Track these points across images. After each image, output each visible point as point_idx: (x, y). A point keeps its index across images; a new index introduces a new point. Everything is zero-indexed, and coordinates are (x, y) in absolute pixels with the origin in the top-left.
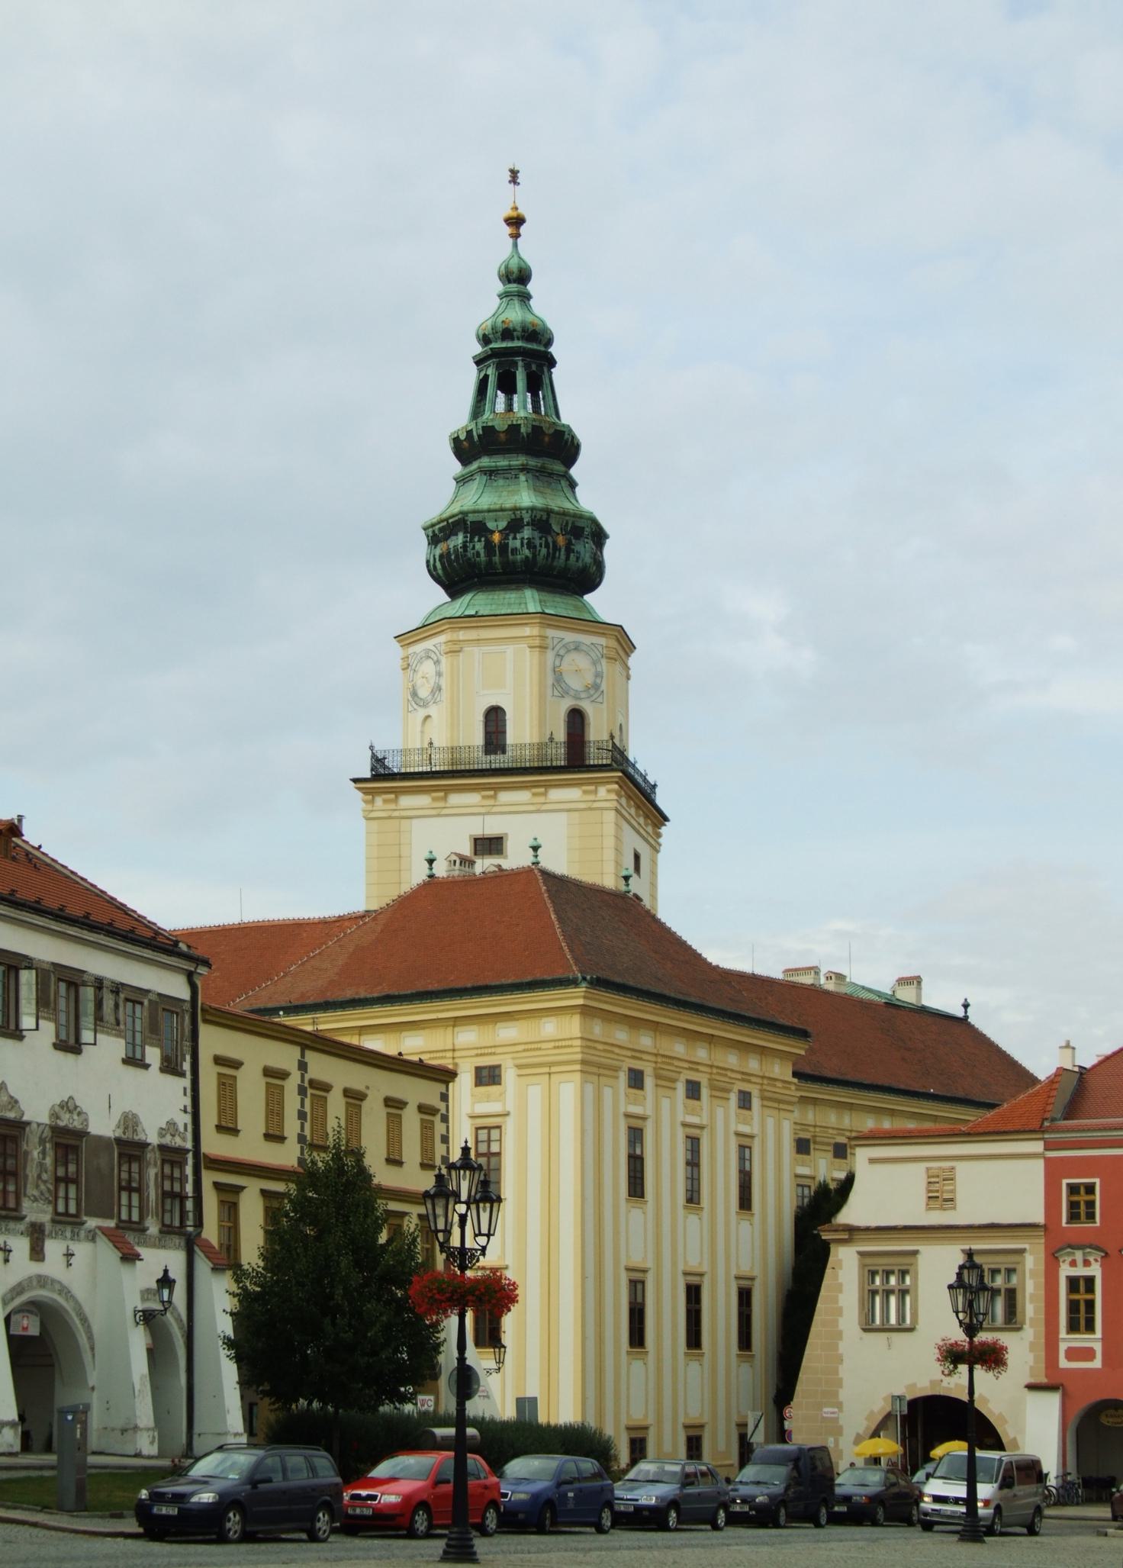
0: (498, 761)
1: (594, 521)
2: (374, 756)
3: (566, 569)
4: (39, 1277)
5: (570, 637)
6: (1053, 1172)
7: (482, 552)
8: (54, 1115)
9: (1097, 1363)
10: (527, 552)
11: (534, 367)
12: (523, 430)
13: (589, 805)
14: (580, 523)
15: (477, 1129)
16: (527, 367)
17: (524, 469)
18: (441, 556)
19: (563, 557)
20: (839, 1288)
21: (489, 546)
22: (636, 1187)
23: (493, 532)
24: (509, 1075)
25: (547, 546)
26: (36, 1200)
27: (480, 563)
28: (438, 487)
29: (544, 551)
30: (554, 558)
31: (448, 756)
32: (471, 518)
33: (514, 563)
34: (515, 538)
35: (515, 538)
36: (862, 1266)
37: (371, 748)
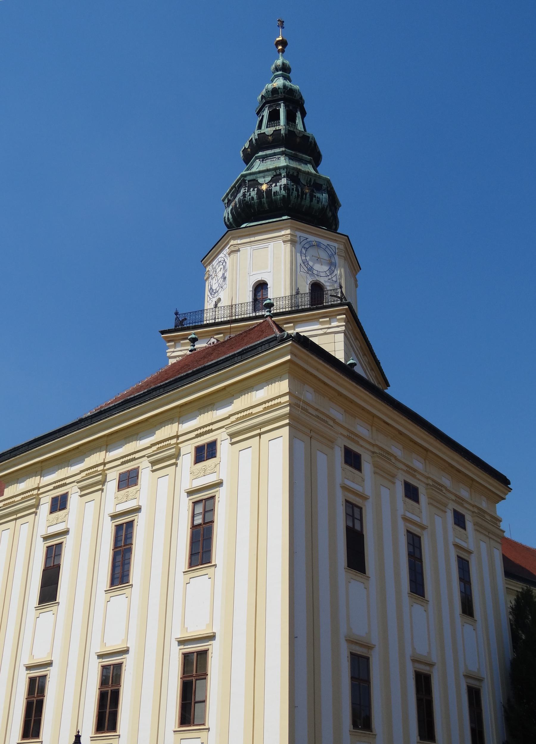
1: (328, 182)
2: (177, 318)
10: (283, 192)
11: (291, 108)
12: (283, 132)
13: (325, 330)
14: (321, 182)
15: (195, 503)
16: (286, 106)
17: (282, 153)
18: (231, 210)
21: (260, 192)
22: (356, 560)
23: (262, 184)
25: (297, 190)
29: (295, 193)
30: (302, 198)
32: (248, 178)
33: (276, 201)
35: (276, 186)
37: (176, 314)
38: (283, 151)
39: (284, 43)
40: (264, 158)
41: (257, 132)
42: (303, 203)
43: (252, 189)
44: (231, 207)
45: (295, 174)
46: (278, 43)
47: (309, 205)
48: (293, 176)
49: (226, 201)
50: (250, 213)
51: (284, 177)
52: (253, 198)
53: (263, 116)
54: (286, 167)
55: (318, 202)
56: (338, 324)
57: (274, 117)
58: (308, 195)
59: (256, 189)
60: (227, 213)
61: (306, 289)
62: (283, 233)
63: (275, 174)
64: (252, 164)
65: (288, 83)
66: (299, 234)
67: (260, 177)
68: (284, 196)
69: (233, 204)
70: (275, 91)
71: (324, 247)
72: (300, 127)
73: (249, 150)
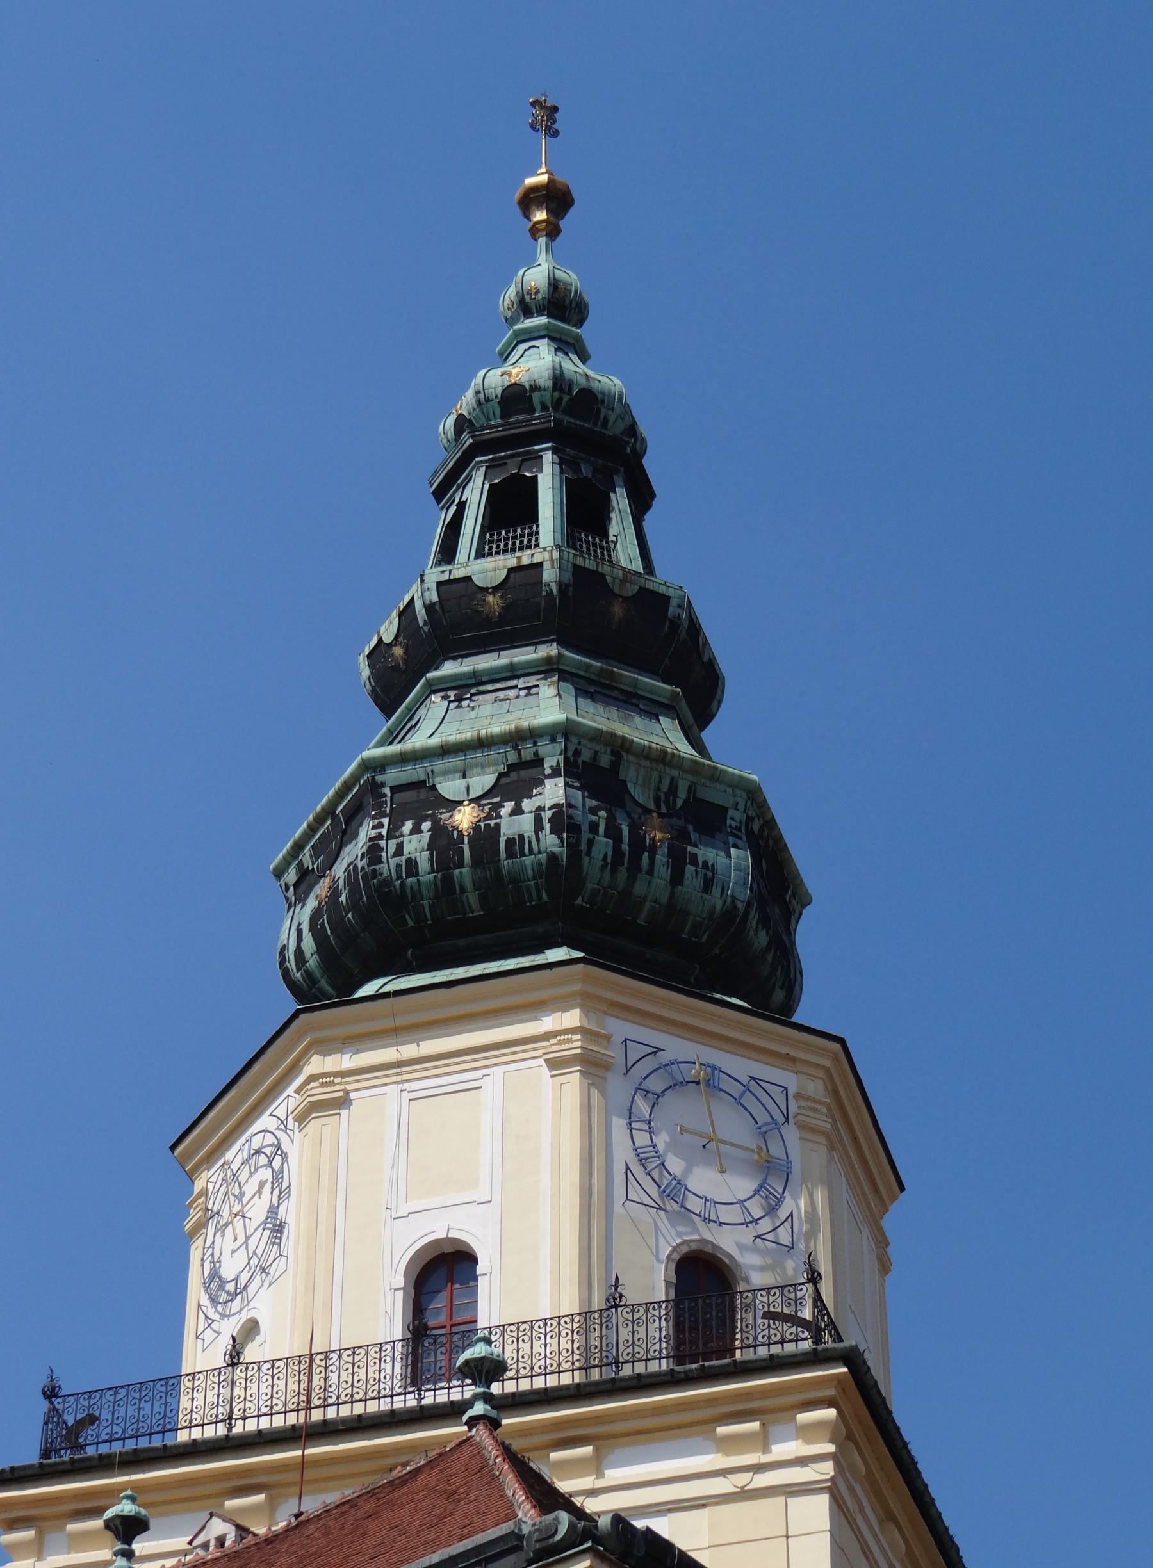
1: (753, 795)
3: (673, 909)
7: (423, 860)
10: (550, 841)
12: (549, 575)
13: (741, 1479)
16: (565, 464)
17: (547, 668)
18: (315, 916)
19: (663, 871)
21: (444, 842)
23: (454, 805)
25: (613, 832)
27: (417, 894)
31: (288, 1387)
32: (393, 776)
33: (516, 879)
34: (517, 811)
35: (517, 811)
37: (51, 1393)
38: (548, 660)
39: (556, 198)
40: (463, 689)
41: (434, 575)
42: (639, 888)
43: (408, 826)
44: (311, 904)
45: (605, 761)
46: (530, 199)
47: (664, 900)
48: (597, 768)
49: (291, 876)
50: (399, 933)
51: (555, 773)
52: (412, 864)
53: (462, 506)
54: (566, 731)
55: (708, 884)
56: (805, 1449)
57: (511, 510)
58: (661, 857)
59: (426, 826)
60: (294, 928)
61: (651, 1282)
62: (548, 1023)
63: (512, 758)
64: (411, 713)
65: (572, 366)
66: (619, 1028)
67: (446, 773)
68: (552, 857)
69: (321, 889)
70: (516, 398)
71: (736, 1089)
72: (626, 554)
73: (398, 651)
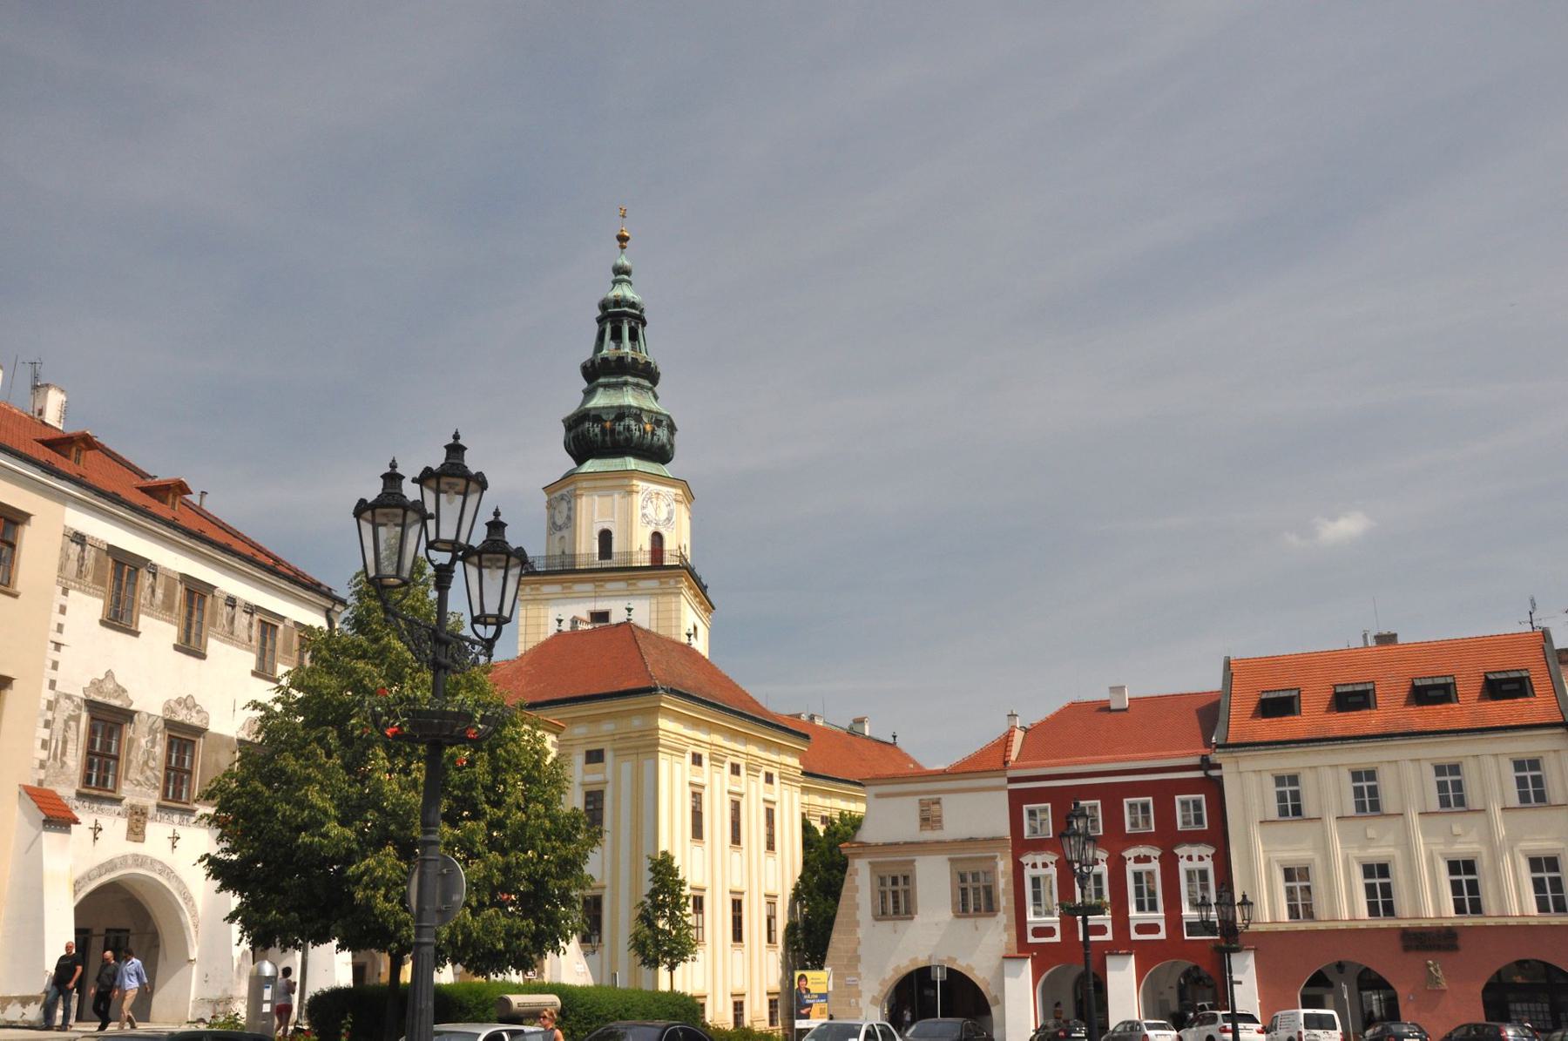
0: (606, 564)
3: (651, 445)
4: (136, 857)
5: (654, 487)
6: (1017, 800)
8: (168, 707)
9: (1057, 938)
20: (856, 889)
21: (603, 429)
24: (608, 756)
26: (139, 784)
28: (570, 395)
36: (873, 871)
40: (606, 386)
